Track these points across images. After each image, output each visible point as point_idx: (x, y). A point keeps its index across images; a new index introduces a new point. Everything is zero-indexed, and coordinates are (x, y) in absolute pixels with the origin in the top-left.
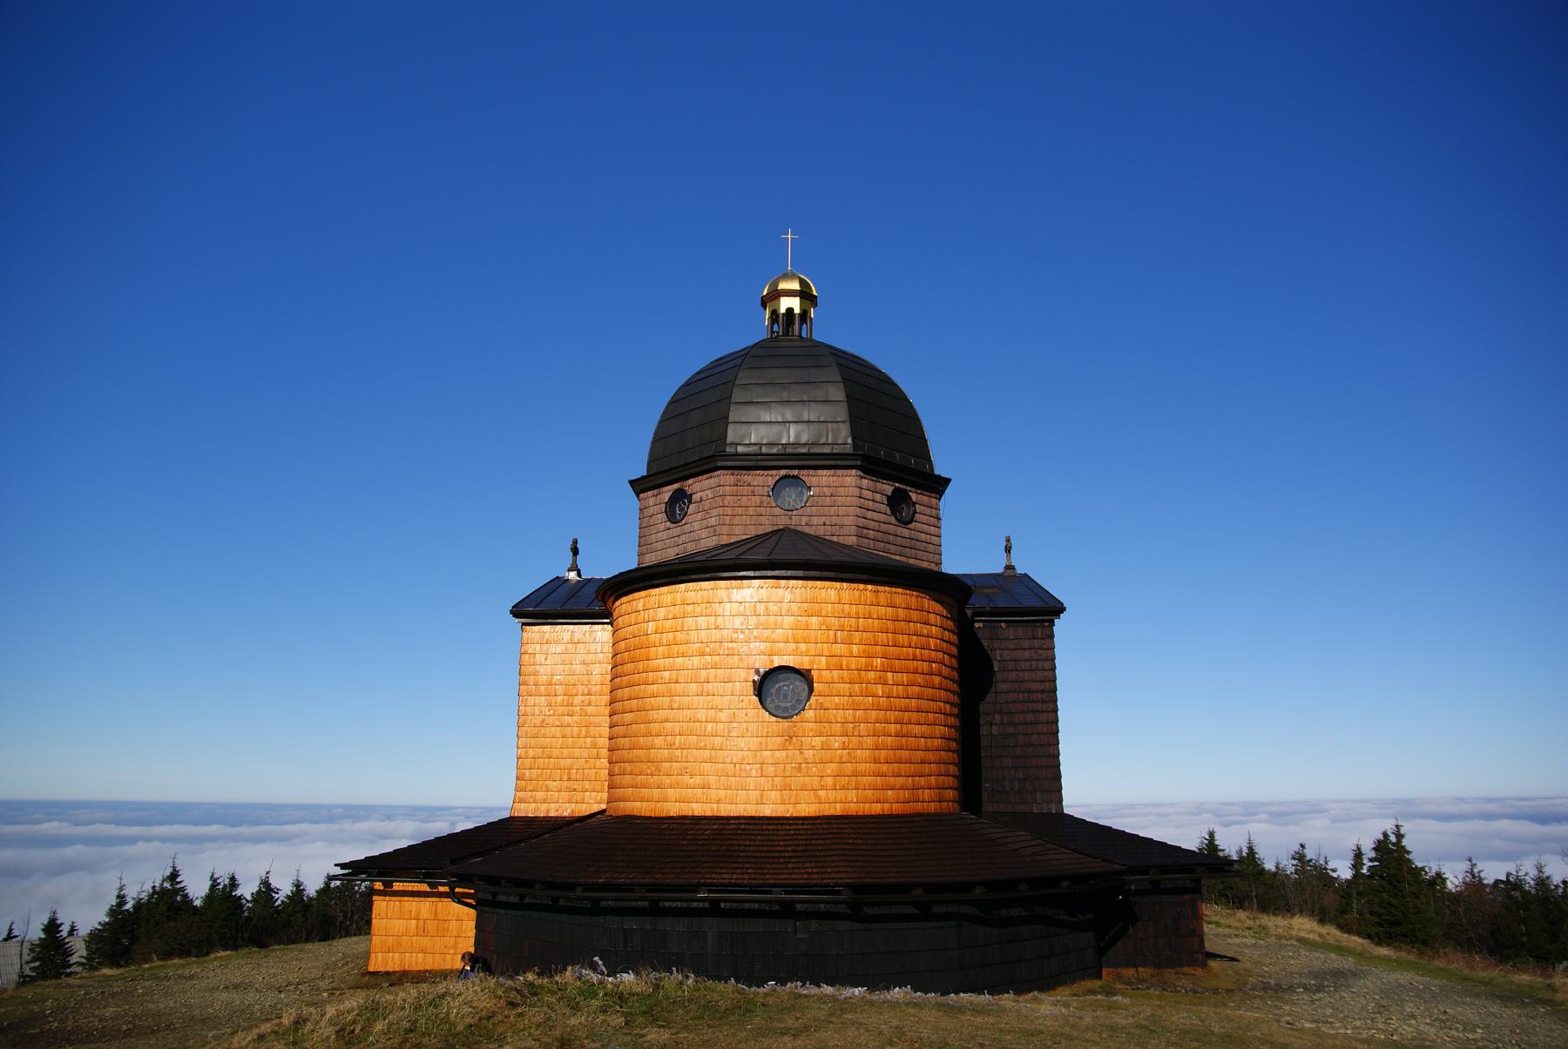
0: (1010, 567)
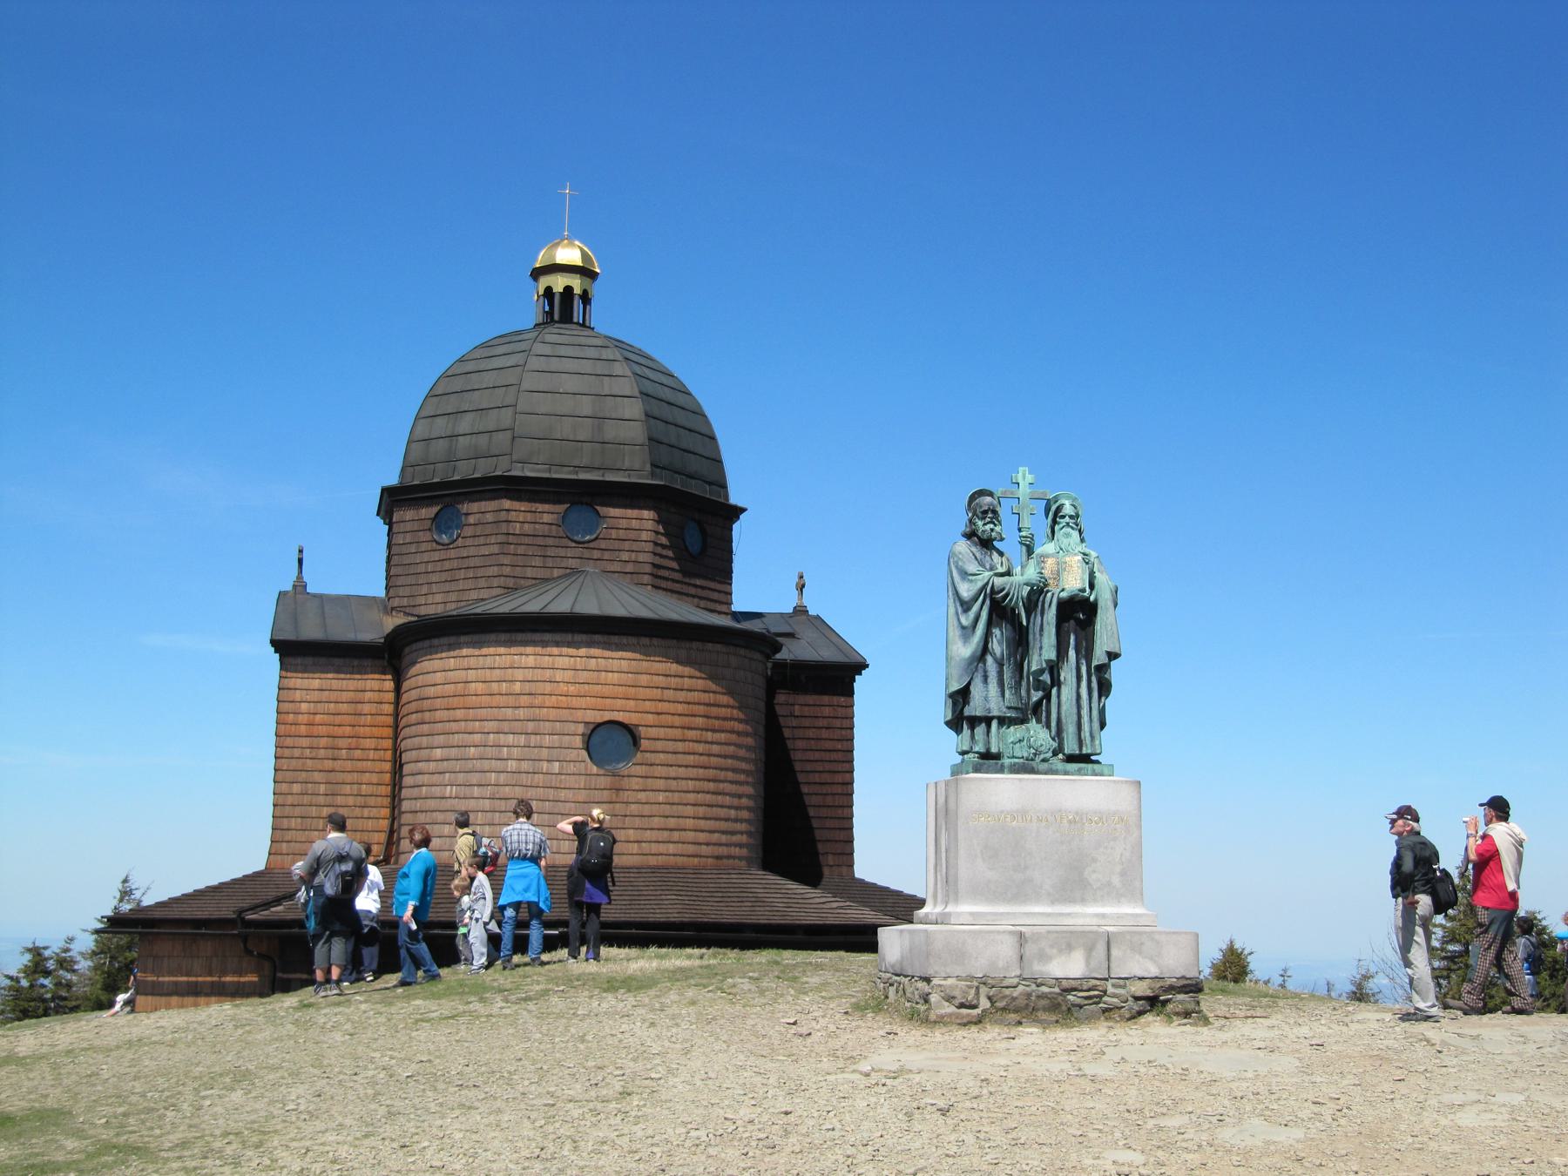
0: (800, 611)
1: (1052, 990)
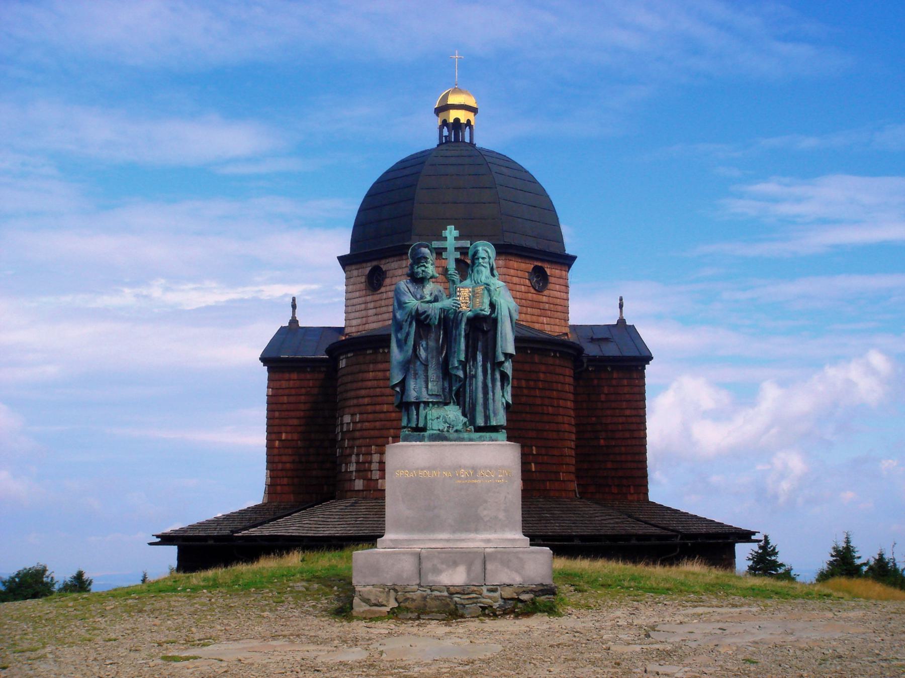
0: (622, 321)
1: (442, 594)
